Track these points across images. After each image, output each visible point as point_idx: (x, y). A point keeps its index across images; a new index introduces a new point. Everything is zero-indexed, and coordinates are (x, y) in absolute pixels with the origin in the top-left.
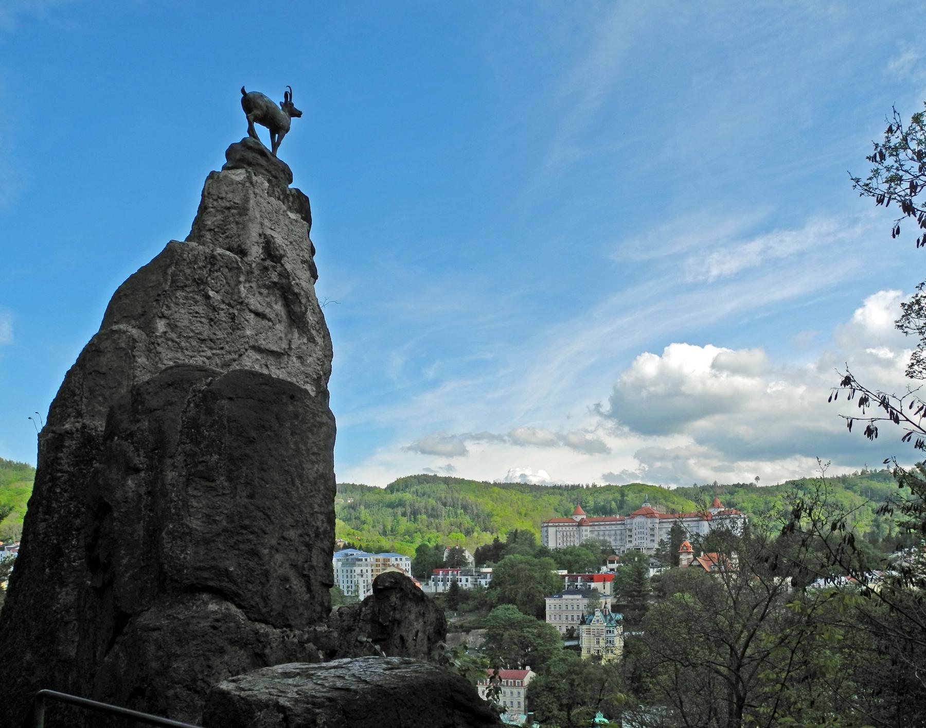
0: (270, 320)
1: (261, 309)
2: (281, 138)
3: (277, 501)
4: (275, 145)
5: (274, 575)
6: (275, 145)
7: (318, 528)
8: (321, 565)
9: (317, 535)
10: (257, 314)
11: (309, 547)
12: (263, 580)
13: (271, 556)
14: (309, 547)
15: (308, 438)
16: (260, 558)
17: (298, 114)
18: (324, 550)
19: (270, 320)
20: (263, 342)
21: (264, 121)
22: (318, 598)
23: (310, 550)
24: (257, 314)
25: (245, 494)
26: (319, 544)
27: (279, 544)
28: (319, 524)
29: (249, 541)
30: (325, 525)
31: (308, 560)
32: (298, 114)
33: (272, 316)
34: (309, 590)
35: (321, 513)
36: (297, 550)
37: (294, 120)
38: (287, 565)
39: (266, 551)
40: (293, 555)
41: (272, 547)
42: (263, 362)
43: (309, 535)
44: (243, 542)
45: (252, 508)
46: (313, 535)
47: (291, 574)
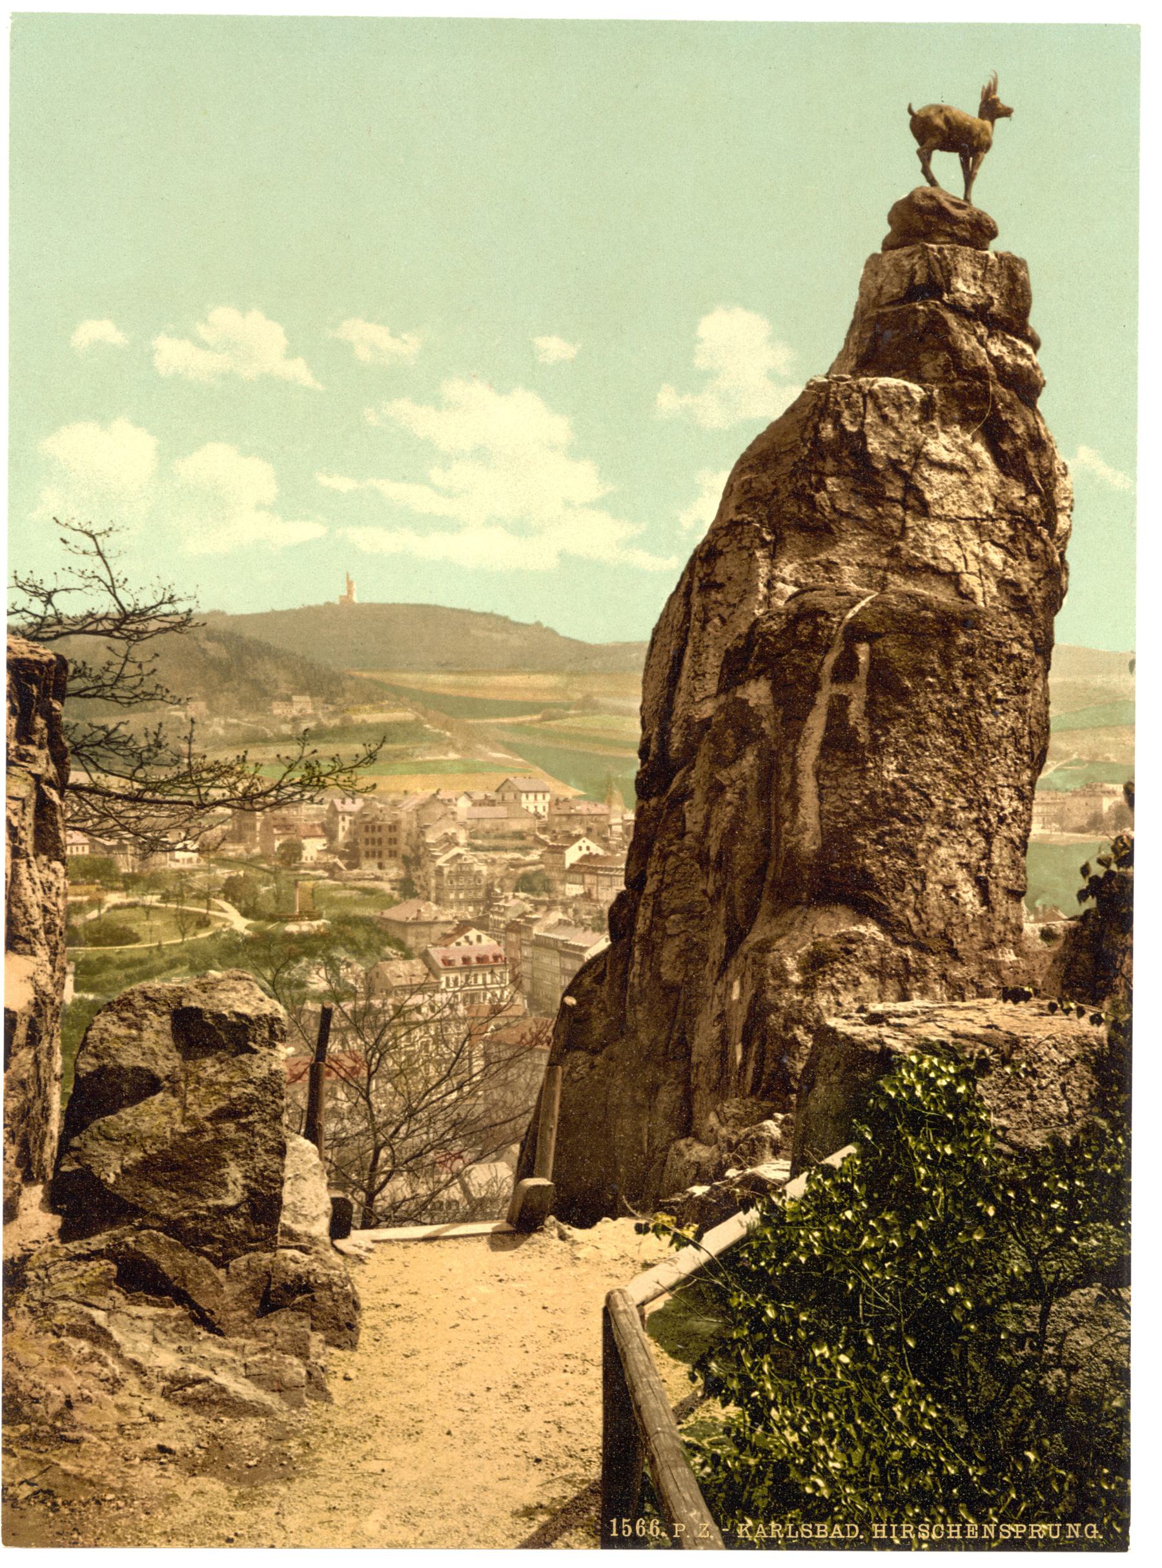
0: (962, 471)
1: (946, 457)
2: (976, 164)
3: (941, 775)
4: (969, 178)
5: (934, 878)
6: (969, 178)
7: (1002, 809)
8: (1007, 862)
9: (1002, 820)
10: (942, 466)
11: (988, 837)
12: (918, 886)
13: (929, 852)
14: (988, 837)
15: (990, 680)
16: (913, 856)
17: (1007, 113)
18: (1012, 841)
19: (962, 471)
20: (955, 508)
21: (948, 145)
22: (1001, 911)
23: (989, 842)
24: (942, 466)
25: (892, 767)
26: (1004, 831)
27: (942, 835)
28: (1005, 803)
29: (898, 831)
30: (1015, 803)
31: (987, 855)
32: (1007, 113)
33: (968, 464)
34: (986, 900)
35: (1008, 786)
36: (969, 843)
37: (999, 122)
38: (953, 863)
39: (921, 846)
40: (962, 849)
41: (930, 840)
42: (952, 537)
43: (988, 821)
44: (890, 834)
45: (903, 785)
46: (993, 820)
47: (960, 875)
